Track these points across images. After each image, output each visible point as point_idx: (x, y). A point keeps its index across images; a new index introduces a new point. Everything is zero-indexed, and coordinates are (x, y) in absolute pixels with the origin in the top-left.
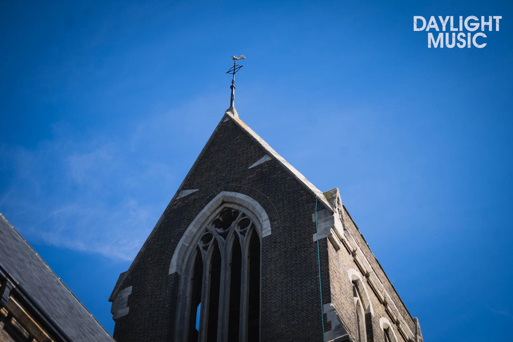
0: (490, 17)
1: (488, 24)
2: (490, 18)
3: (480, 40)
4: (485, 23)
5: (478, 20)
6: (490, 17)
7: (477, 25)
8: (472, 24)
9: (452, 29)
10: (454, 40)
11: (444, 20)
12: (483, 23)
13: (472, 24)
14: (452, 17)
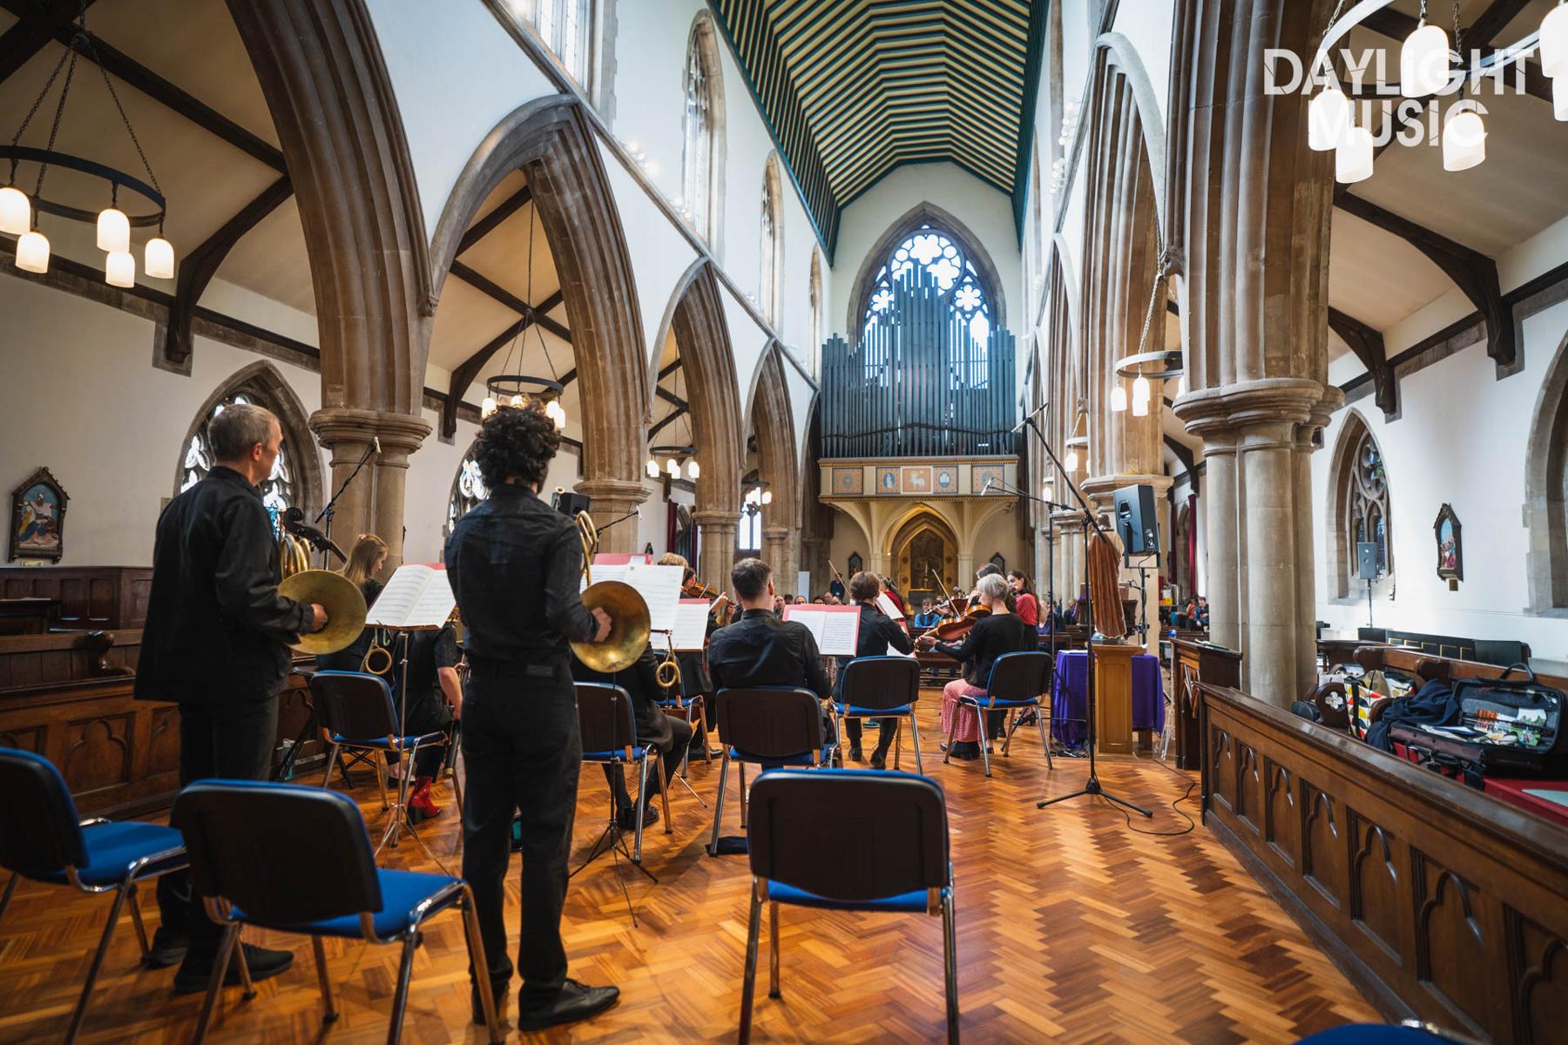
11: (1357, 61)
14: (1381, 53)
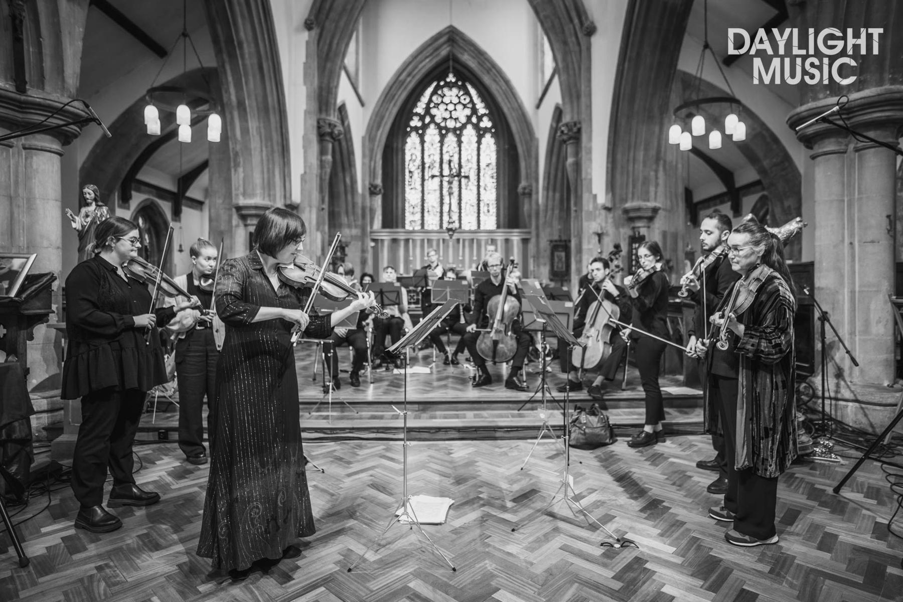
0: (862, 29)
1: (858, 42)
2: (863, 32)
3: (844, 71)
4: (854, 41)
5: (838, 33)
6: (862, 29)
7: (840, 44)
8: (830, 43)
9: (796, 51)
10: (799, 70)
12: (851, 41)
13: (830, 43)
